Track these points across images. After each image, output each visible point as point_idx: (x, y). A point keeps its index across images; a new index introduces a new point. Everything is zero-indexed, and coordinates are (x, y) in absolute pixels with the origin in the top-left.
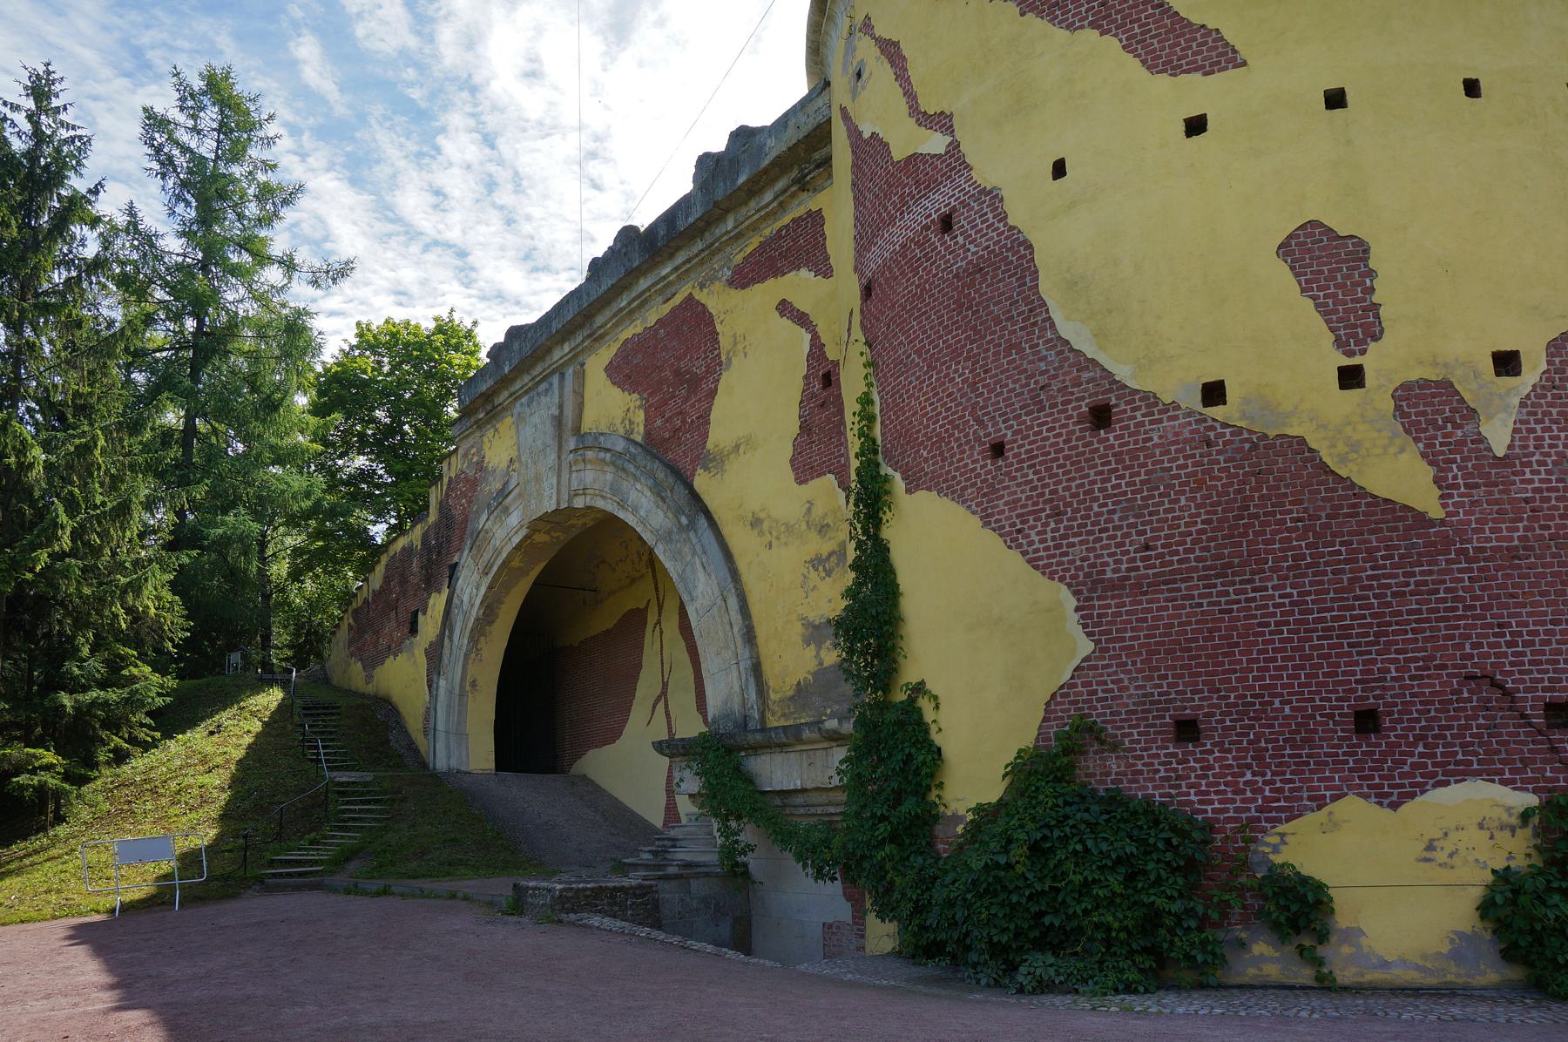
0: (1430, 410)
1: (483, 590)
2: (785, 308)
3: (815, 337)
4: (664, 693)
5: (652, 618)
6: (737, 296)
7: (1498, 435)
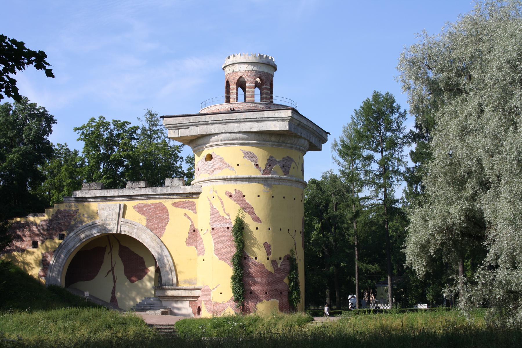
2: (185, 215)
3: (192, 223)
4: (113, 269)
5: (108, 250)
7: (279, 266)
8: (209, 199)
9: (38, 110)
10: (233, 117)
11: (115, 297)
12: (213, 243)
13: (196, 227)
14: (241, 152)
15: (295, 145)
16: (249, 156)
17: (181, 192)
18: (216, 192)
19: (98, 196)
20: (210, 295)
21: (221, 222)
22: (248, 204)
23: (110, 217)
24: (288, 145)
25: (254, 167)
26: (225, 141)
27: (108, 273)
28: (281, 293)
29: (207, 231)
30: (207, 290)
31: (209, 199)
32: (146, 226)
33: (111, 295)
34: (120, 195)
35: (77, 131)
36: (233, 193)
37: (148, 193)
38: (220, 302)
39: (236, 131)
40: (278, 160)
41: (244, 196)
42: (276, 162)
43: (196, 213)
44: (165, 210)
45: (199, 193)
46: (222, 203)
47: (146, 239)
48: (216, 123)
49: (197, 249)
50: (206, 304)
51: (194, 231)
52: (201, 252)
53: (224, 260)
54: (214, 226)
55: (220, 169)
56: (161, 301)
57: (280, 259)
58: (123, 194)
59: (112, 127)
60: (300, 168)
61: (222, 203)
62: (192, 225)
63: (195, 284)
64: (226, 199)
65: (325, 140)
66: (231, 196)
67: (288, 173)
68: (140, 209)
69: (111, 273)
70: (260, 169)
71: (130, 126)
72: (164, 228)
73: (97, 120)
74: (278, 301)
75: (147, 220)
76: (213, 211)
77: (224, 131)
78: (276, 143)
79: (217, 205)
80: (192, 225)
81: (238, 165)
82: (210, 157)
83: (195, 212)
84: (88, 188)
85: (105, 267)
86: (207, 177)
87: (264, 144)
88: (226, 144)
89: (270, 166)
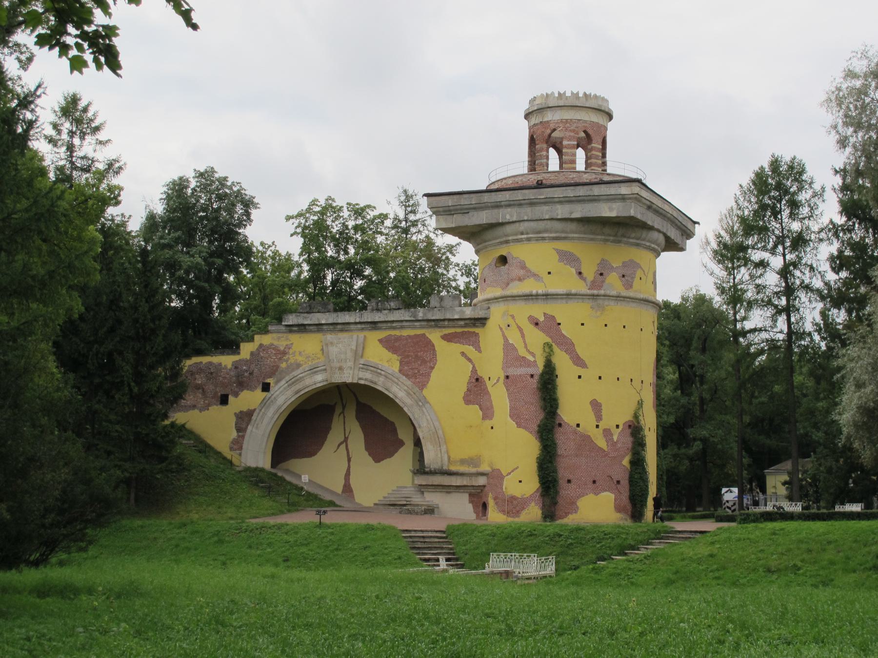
0: (607, 433)
1: (293, 399)
2: (463, 354)
3: (474, 367)
5: (338, 410)
6: (444, 343)
8: (501, 329)
9: (230, 188)
10: (540, 195)
11: (350, 485)
12: (508, 401)
13: (480, 373)
14: (554, 252)
15: (644, 240)
16: (567, 258)
17: (456, 317)
18: (513, 317)
19: (323, 322)
20: (502, 485)
21: (521, 366)
22: (564, 336)
23: (343, 356)
24: (631, 240)
25: (576, 277)
26: (527, 234)
27: (339, 446)
28: (618, 482)
29: (498, 381)
30: (496, 476)
31: (501, 329)
32: (400, 371)
33: (343, 482)
34: (358, 320)
35: (291, 221)
36: (542, 319)
37: (402, 318)
38: (518, 494)
39: (547, 217)
41: (559, 324)
42: (612, 269)
43: (480, 351)
44: (429, 346)
45: (486, 319)
46: (523, 336)
47: (399, 391)
48: (514, 205)
49: (481, 409)
50: (495, 499)
51: (477, 380)
52: (488, 413)
53: (525, 428)
54: (512, 372)
55: (520, 280)
56: (423, 493)
57: (617, 426)
58: (362, 321)
59: (346, 213)
60: (650, 279)
61: (523, 336)
62: (474, 371)
63: (476, 465)
64: (529, 328)
65: (688, 234)
66: (537, 324)
67: (631, 287)
68: (389, 344)
69: (344, 445)
70: (584, 279)
71: (376, 213)
72: (428, 375)
73: (322, 202)
74: (612, 496)
75: (401, 362)
76: (508, 348)
77: (526, 218)
78: (612, 238)
79: (514, 338)
80: (474, 371)
81: (549, 273)
82: (503, 260)
83: (479, 349)
84: (308, 310)
85: (335, 436)
86: (498, 292)
87: (592, 239)
88: (529, 239)
89: (601, 274)
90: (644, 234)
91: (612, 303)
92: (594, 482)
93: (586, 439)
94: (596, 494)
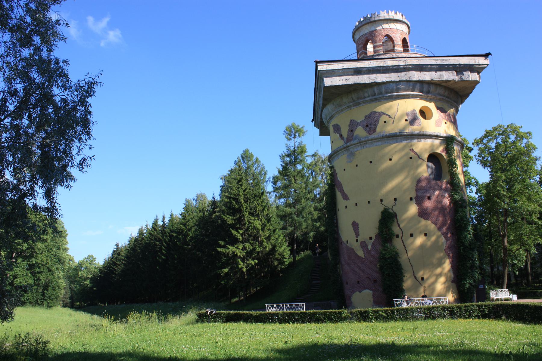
0: (363, 245)
7: (369, 247)
24: (366, 99)
40: (359, 121)
42: (358, 124)
57: (371, 238)
67: (375, 131)
74: (371, 292)
87: (342, 111)
90: (376, 89)
91: (359, 148)
92: (358, 282)
93: (352, 250)
94: (360, 292)
